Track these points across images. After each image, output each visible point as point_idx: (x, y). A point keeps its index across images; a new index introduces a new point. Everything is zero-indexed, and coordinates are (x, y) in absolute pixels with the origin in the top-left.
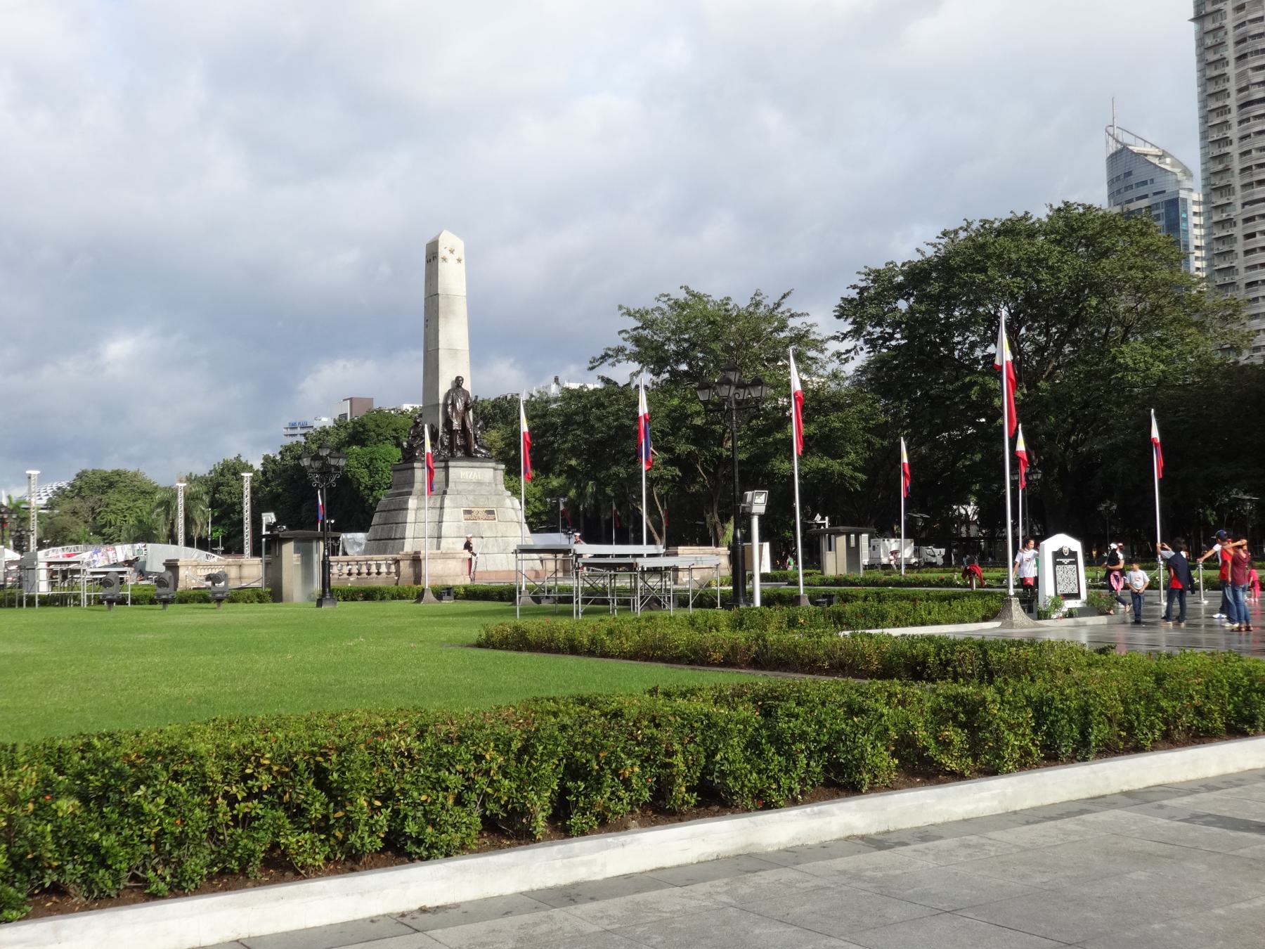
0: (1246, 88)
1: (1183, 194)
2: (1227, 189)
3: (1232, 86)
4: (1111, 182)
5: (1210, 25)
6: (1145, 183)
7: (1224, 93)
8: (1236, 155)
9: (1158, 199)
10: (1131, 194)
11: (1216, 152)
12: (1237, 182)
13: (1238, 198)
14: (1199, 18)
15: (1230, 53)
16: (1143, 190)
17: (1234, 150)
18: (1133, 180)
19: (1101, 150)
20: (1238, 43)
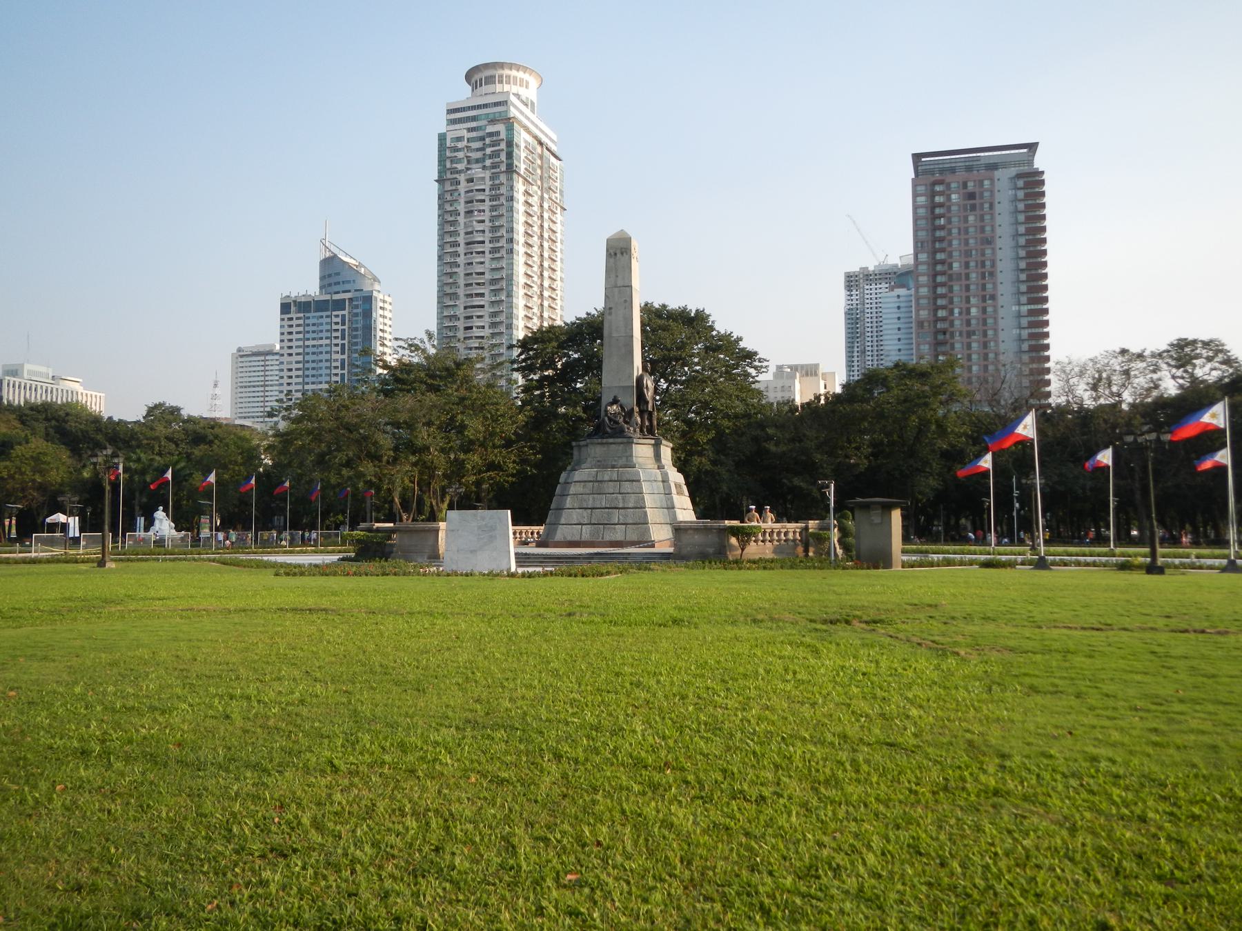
0: (471, 233)
1: (375, 294)
2: (454, 296)
3: (461, 229)
4: (322, 278)
5: (448, 187)
6: (349, 282)
7: (455, 233)
8: (462, 275)
9: (358, 294)
10: (336, 288)
11: (449, 271)
12: (461, 292)
13: (461, 302)
14: (440, 181)
15: (461, 208)
16: (347, 287)
17: (461, 271)
18: (340, 279)
19: (318, 256)
20: (467, 202)
